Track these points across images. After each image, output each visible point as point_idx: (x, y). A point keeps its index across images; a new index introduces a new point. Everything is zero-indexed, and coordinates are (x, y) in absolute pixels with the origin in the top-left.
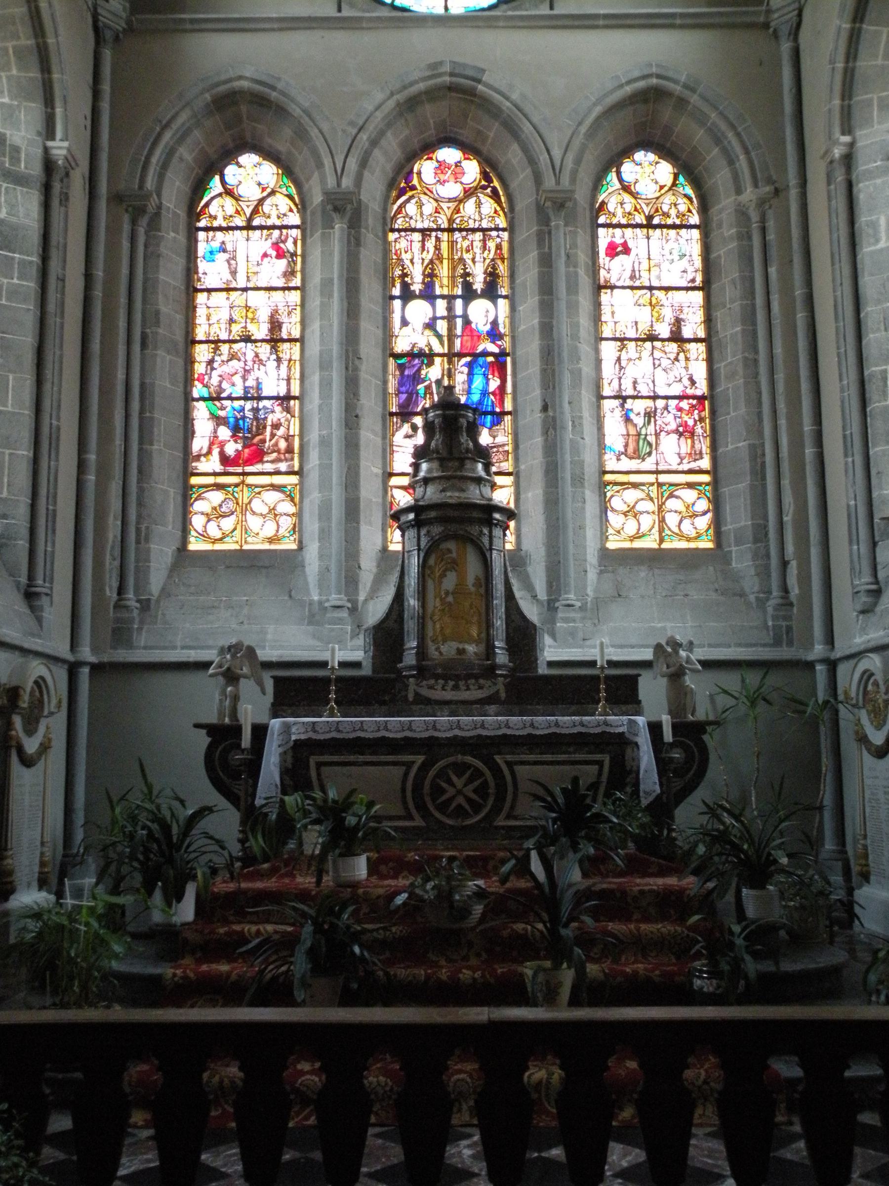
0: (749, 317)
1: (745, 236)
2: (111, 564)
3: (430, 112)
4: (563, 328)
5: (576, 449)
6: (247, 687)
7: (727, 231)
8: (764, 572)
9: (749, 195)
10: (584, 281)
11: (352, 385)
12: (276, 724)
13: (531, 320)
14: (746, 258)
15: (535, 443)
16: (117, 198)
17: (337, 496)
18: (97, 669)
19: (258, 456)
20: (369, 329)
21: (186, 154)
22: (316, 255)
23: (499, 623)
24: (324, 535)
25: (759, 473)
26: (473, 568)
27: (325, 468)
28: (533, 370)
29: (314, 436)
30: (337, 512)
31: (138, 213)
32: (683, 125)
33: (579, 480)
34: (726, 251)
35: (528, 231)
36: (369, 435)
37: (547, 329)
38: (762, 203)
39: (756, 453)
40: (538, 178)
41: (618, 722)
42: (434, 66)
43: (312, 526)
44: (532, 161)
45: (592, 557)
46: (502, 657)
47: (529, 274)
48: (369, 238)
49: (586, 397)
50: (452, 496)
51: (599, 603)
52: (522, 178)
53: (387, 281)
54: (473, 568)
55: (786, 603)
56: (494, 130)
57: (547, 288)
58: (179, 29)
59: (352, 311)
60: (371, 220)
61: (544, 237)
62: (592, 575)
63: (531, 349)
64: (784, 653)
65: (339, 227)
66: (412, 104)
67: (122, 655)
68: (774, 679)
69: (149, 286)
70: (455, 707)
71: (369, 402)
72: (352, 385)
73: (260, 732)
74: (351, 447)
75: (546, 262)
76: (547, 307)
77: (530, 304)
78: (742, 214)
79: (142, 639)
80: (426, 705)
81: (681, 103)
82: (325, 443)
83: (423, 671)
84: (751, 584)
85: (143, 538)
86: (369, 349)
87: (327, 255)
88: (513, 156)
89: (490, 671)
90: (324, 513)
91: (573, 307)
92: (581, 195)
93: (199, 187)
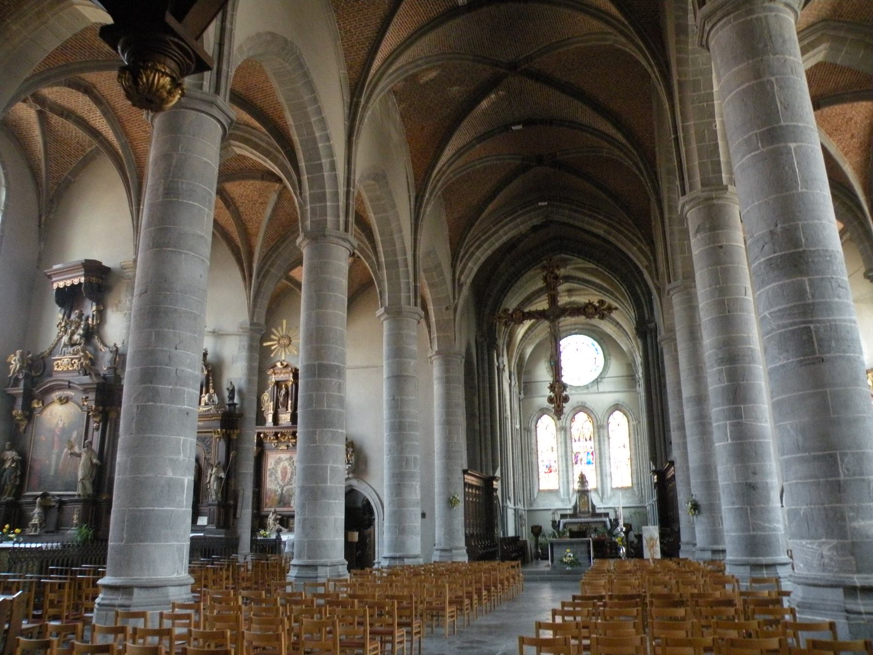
0: (635, 446)
1: (634, 430)
2: (528, 493)
3: (578, 409)
4: (603, 450)
5: (605, 470)
6: (556, 515)
7: (632, 428)
8: (638, 490)
9: (634, 423)
10: (606, 439)
11: (567, 460)
12: (562, 521)
13: (597, 447)
14: (634, 433)
15: (599, 469)
16: (524, 429)
17: (565, 480)
18: (528, 511)
19: (551, 472)
20: (569, 449)
21: (535, 418)
22: (559, 436)
23: (590, 506)
24: (563, 487)
25: (637, 473)
26: (586, 499)
27: (563, 475)
28: (598, 456)
29: (561, 469)
30: (565, 483)
31: (528, 431)
32: (623, 409)
33: (606, 476)
34: (632, 431)
35: (596, 430)
36: (570, 469)
37: (600, 449)
38: (637, 425)
39: (637, 470)
40: (597, 421)
41: (604, 519)
42: (578, 402)
43: (561, 485)
44: (596, 417)
45: (609, 489)
46: (590, 510)
47: (597, 438)
48: (568, 433)
49: (607, 460)
50: (583, 489)
51: (610, 497)
52: (594, 420)
53: (571, 439)
54: (586, 499)
55: (642, 496)
56: (589, 412)
57: (599, 442)
58: (533, 397)
59: (566, 447)
60: (568, 429)
61: (599, 432)
62: (609, 492)
63: (597, 452)
64: (641, 505)
65: (563, 432)
66: (574, 409)
67: (531, 508)
68: (639, 510)
69: (531, 443)
70: (584, 518)
71: (570, 463)
72: (567, 460)
73: (559, 522)
74: (567, 471)
75: (599, 436)
76: (600, 444)
77: (597, 444)
78: (634, 425)
79: (535, 505)
80: (580, 517)
81: (622, 406)
82: (563, 471)
83: (580, 512)
84: (637, 493)
85: (533, 488)
86: (569, 453)
87: (561, 437)
88: (593, 416)
89: (589, 512)
90: (563, 483)
91: (604, 445)
92: (605, 424)
93: (537, 423)
